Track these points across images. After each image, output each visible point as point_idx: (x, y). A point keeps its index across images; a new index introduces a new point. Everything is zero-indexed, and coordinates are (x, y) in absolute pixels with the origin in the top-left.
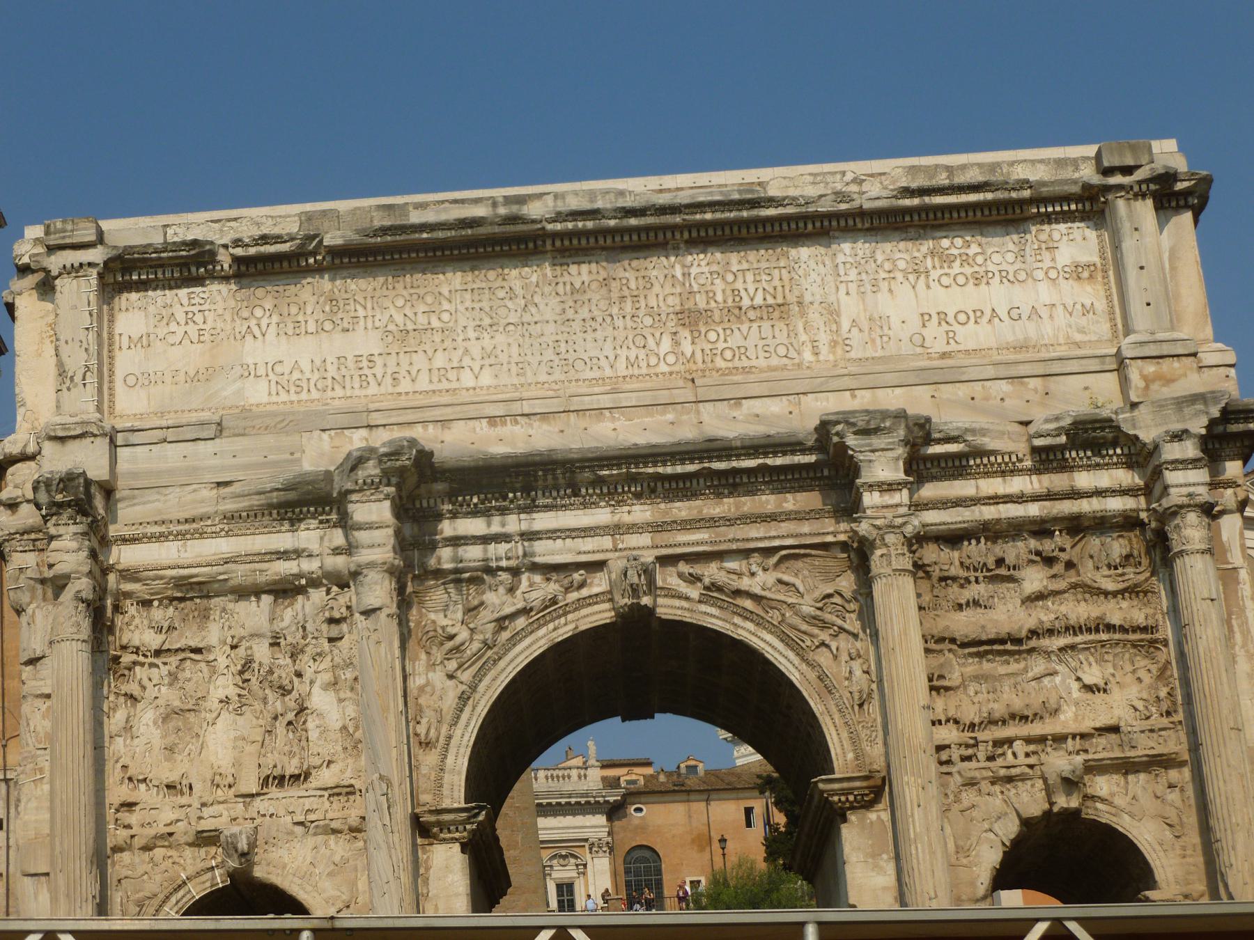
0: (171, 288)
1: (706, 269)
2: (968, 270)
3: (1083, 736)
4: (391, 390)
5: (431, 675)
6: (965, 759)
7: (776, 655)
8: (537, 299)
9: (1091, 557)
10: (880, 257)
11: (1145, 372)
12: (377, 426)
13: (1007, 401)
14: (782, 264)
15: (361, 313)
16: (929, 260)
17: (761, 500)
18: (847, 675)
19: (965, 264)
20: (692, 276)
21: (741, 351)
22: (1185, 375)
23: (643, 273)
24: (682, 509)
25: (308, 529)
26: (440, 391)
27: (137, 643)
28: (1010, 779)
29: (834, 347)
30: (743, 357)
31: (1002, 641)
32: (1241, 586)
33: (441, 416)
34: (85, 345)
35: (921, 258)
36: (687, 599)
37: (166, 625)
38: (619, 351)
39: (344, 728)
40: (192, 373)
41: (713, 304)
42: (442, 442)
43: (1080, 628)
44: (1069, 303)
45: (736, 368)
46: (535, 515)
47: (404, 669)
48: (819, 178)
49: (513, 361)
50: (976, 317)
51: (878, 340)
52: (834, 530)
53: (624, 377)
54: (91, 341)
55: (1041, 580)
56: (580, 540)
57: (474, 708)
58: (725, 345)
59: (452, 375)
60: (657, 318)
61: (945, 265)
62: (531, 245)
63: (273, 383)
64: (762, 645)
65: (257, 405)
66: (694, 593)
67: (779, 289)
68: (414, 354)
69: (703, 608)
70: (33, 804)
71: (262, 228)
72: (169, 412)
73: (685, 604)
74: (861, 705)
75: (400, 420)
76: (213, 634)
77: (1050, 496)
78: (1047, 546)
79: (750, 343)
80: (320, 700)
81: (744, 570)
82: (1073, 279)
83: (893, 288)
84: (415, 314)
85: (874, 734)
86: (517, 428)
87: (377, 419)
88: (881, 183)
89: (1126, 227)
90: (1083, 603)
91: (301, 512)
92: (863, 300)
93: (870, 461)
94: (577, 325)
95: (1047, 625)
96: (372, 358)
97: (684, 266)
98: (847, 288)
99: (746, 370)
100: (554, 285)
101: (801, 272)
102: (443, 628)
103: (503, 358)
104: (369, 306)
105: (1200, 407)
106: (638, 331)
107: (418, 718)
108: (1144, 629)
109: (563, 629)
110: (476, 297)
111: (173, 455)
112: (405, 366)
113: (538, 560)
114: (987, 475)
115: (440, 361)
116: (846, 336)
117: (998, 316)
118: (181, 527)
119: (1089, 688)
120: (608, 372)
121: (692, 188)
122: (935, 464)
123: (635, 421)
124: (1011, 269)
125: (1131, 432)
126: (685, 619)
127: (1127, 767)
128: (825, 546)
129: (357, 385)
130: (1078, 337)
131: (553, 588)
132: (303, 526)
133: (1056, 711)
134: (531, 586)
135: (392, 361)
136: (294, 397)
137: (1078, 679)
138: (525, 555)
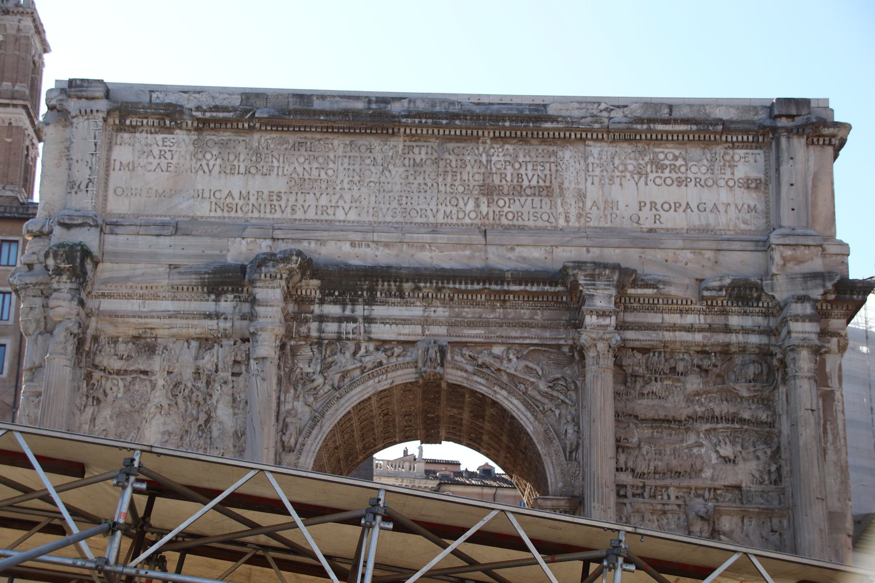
0: (151, 133)
1: (502, 159)
2: (674, 176)
3: (715, 489)
4: (290, 216)
5: (295, 403)
6: (634, 495)
7: (519, 414)
8: (391, 167)
9: (735, 372)
10: (617, 162)
11: (785, 255)
12: (278, 239)
13: (689, 264)
14: (552, 160)
15: (276, 164)
16: (649, 166)
17: (520, 312)
18: (564, 432)
19: (673, 171)
20: (493, 162)
21: (518, 215)
22: (812, 259)
23: (461, 157)
24: (469, 312)
25: (226, 301)
26: (322, 221)
27: (105, 363)
28: (664, 513)
29: (580, 218)
30: (519, 218)
31: (669, 421)
32: (836, 403)
33: (321, 236)
34: (90, 165)
35: (644, 165)
36: (466, 371)
38: (440, 207)
39: (236, 432)
40: (160, 191)
41: (504, 182)
42: (320, 254)
43: (722, 418)
44: (740, 203)
45: (514, 226)
46: (374, 307)
47: (279, 398)
48: (583, 105)
49: (371, 206)
50: (675, 207)
51: (609, 217)
52: (564, 337)
53: (442, 224)
54: (94, 163)
55: (699, 384)
56: (401, 326)
57: (321, 427)
58: (509, 210)
59: (331, 211)
60: (467, 188)
61: (660, 171)
62: (390, 131)
63: (213, 204)
64: (511, 406)
65: (202, 217)
66: (470, 368)
67: (548, 176)
68: (307, 195)
69: (476, 378)
71: (216, 100)
72: (143, 216)
74: (571, 453)
75: (293, 236)
76: (156, 364)
77: (711, 329)
79: (525, 210)
80: (223, 413)
81: (505, 356)
82: (745, 188)
83: (623, 183)
84: (311, 169)
85: (577, 472)
86: (368, 250)
87: (278, 234)
88: (623, 113)
89: (785, 156)
90: (725, 403)
91: (223, 289)
92: (602, 189)
93: (593, 295)
94: (414, 187)
95: (699, 414)
96: (280, 194)
97: (488, 155)
98: (593, 180)
99: (521, 228)
100: (402, 159)
101: (564, 167)
102: (307, 374)
103: (365, 203)
104: (281, 160)
105: (819, 281)
106: (454, 195)
107: (284, 431)
109: (383, 383)
110: (352, 162)
111: (144, 243)
112: (301, 202)
113: (373, 336)
114: (670, 311)
115: (324, 200)
116: (588, 211)
117: (690, 208)
118: (144, 291)
120: (431, 220)
121: (499, 104)
122: (637, 300)
123: (445, 253)
124: (703, 178)
125: (770, 294)
126: (463, 384)
128: (559, 347)
129: (268, 211)
130: (743, 227)
131: (381, 356)
132: (223, 299)
133: (701, 471)
134: (366, 352)
135: (292, 198)
136: (226, 214)
137: (717, 452)
138: (365, 332)
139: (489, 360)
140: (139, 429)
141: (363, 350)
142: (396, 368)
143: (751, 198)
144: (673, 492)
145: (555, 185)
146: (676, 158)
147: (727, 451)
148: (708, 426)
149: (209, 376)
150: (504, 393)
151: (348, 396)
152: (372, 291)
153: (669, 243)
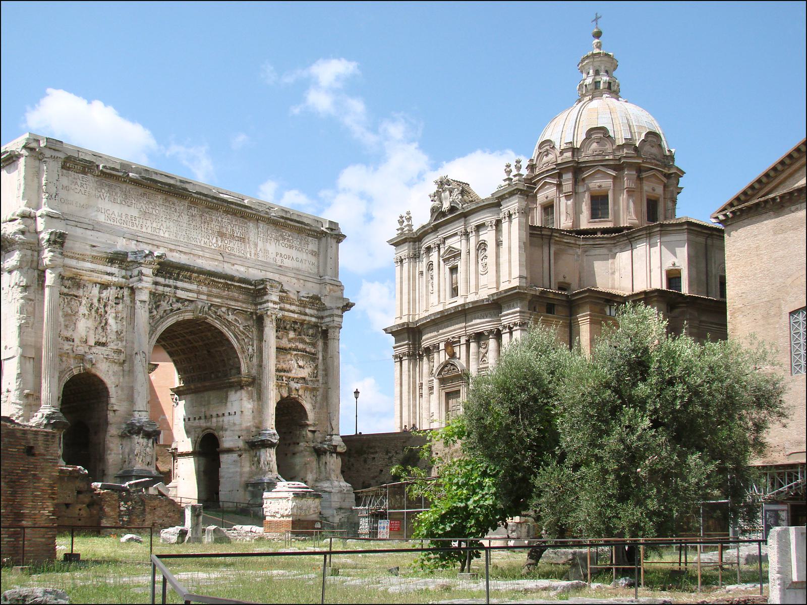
2: (289, 244)
10: (269, 233)
21: (233, 249)
24: (215, 291)
28: (281, 386)
36: (212, 317)
37: (68, 285)
39: (117, 332)
52: (250, 308)
66: (214, 316)
69: (216, 321)
70: (25, 334)
73: (212, 319)
75: (146, 241)
76: (80, 293)
78: (296, 326)
79: (236, 246)
80: (111, 321)
89: (329, 246)
99: (234, 255)
108: (313, 354)
114: (287, 303)
119: (300, 367)
127: (306, 389)
128: (247, 312)
130: (310, 271)
131: (179, 305)
137: (298, 363)
139: (222, 314)
140: (75, 324)
141: (171, 301)
142: (186, 311)
143: (313, 259)
144: (284, 378)
145: (247, 238)
146: (289, 236)
147: (301, 363)
148: (295, 352)
149: (106, 303)
150: (226, 329)
151: (167, 321)
152: (178, 274)
153: (289, 274)
